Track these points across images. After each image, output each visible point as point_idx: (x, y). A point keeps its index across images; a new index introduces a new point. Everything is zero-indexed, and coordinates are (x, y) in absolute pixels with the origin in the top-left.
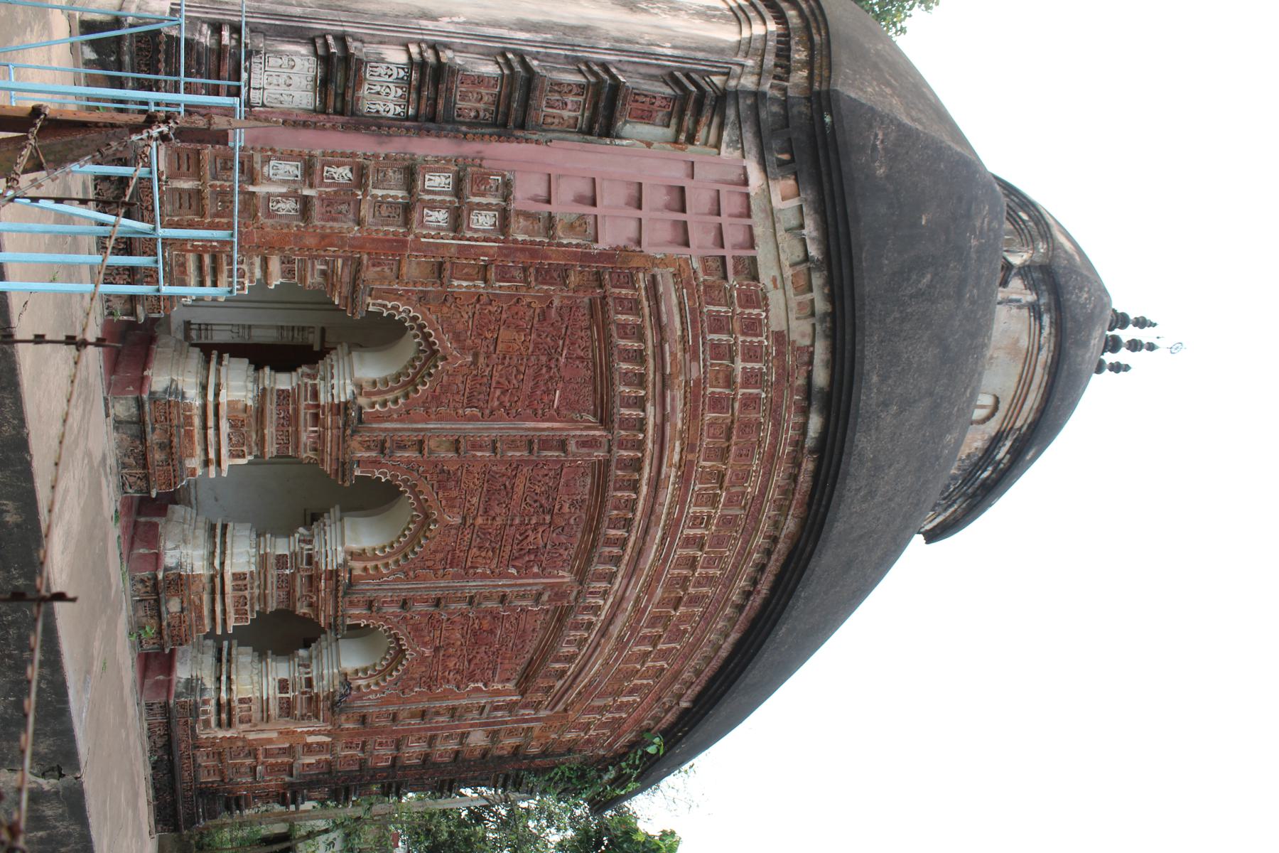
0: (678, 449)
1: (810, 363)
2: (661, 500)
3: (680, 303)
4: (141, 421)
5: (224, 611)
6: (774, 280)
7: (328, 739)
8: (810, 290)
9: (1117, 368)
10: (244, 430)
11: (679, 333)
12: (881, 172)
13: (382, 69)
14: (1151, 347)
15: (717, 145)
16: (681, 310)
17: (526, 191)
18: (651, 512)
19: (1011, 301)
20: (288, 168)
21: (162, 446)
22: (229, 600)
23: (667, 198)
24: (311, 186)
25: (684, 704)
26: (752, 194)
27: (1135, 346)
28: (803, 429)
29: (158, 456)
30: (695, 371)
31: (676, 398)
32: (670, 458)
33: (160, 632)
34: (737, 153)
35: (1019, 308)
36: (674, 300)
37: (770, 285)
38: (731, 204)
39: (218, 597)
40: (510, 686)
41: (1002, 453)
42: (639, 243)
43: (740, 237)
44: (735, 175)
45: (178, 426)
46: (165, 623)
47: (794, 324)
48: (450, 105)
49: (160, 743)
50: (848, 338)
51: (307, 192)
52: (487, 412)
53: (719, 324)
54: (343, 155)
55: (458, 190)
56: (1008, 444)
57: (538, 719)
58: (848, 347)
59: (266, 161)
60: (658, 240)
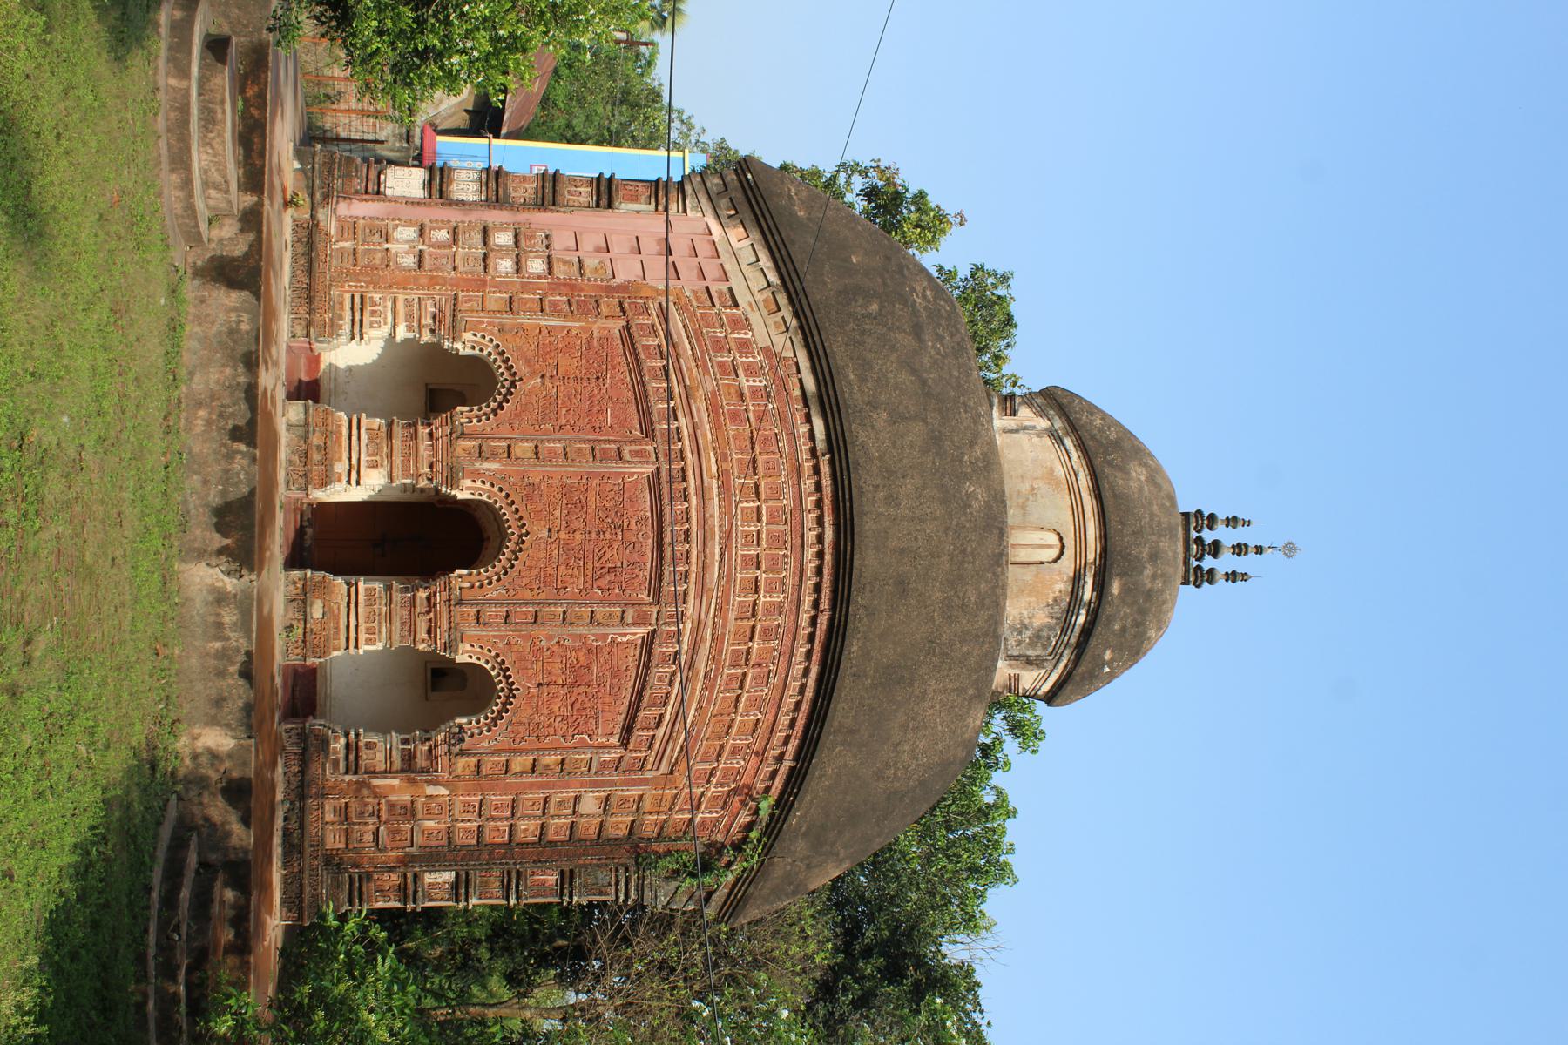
0: (713, 460)
1: (799, 372)
4: (307, 424)
7: (443, 791)
9: (1232, 577)
12: (801, 214)
13: (464, 174)
14: (1259, 550)
15: (685, 211)
17: (563, 241)
18: (704, 521)
19: (1026, 428)
21: (318, 448)
25: (788, 764)
27: (1239, 549)
29: (316, 457)
30: (710, 384)
31: (700, 407)
32: (709, 469)
38: (704, 249)
40: (614, 740)
41: (1087, 593)
43: (717, 273)
44: (701, 228)
47: (774, 338)
48: (507, 195)
50: (817, 338)
53: (719, 346)
55: (517, 244)
56: (1090, 581)
57: (645, 782)
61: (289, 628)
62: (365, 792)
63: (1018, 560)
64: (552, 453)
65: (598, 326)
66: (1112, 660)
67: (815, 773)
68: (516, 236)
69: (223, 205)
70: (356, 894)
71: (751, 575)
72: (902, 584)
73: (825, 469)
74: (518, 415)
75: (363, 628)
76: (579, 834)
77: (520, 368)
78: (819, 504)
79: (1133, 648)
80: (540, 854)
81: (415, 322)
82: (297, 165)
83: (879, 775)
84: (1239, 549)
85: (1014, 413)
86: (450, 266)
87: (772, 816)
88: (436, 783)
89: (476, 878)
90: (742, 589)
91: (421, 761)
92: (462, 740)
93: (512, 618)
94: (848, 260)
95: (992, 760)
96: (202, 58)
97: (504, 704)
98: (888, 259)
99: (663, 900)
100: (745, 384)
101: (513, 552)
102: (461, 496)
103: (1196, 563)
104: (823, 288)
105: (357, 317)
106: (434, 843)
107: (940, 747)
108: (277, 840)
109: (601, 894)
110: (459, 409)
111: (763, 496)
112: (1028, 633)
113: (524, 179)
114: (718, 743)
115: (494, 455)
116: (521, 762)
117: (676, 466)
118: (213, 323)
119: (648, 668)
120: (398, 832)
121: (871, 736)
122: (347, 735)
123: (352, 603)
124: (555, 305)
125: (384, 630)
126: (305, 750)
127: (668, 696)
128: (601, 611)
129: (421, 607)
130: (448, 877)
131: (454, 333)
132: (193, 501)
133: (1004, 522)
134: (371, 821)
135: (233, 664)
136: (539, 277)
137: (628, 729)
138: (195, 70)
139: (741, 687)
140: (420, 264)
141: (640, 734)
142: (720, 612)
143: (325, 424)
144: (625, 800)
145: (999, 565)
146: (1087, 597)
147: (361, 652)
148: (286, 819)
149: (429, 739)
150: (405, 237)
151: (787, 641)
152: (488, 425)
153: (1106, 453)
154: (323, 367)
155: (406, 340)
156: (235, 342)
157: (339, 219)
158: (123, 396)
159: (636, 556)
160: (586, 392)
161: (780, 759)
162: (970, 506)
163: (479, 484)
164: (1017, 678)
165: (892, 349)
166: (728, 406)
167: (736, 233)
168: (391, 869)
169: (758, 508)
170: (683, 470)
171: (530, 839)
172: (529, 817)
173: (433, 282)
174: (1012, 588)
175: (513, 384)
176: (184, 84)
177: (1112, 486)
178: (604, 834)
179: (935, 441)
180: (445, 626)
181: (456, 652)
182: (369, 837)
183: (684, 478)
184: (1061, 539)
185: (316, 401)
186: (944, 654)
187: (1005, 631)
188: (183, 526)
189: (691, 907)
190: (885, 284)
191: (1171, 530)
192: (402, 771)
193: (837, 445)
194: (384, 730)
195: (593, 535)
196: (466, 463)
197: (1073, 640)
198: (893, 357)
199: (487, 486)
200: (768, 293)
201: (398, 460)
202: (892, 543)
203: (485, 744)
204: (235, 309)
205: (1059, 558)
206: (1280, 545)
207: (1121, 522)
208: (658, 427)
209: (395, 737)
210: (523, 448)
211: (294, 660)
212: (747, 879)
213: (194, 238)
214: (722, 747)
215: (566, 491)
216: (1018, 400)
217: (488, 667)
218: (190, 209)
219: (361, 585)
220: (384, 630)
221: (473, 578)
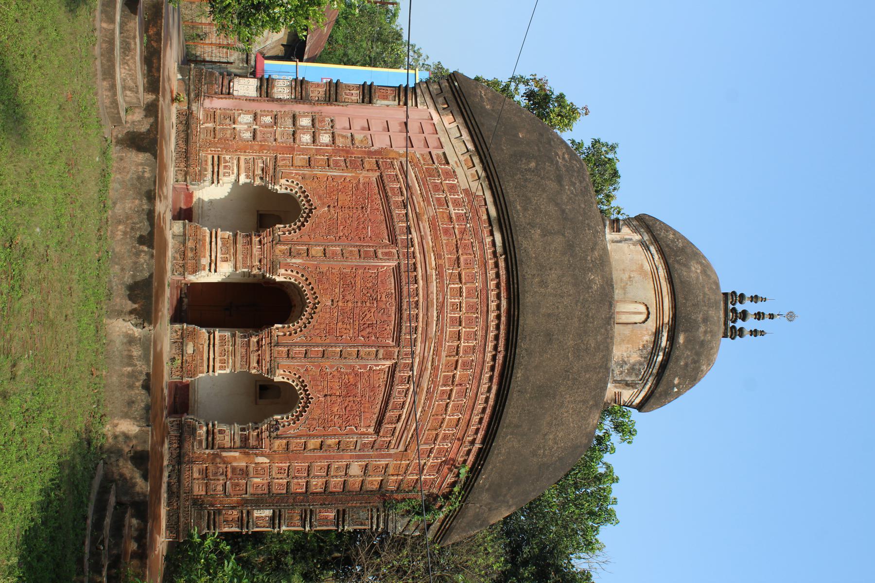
0: (433, 258)
1: (486, 204)
4: (185, 235)
6: (456, 163)
7: (266, 460)
8: (474, 166)
9: (754, 333)
12: (488, 107)
13: (281, 82)
14: (772, 316)
15: (416, 105)
17: (341, 124)
18: (427, 296)
19: (626, 240)
21: (192, 249)
22: (216, 349)
25: (478, 446)
27: (759, 316)
28: (494, 243)
29: (190, 255)
31: (425, 226)
32: (430, 264)
35: (634, 245)
37: (455, 166)
38: (428, 128)
39: (211, 346)
40: (371, 430)
41: (664, 342)
43: (436, 144)
44: (427, 116)
48: (307, 95)
50: (497, 183)
51: (255, 127)
53: (437, 188)
55: (313, 125)
56: (665, 334)
57: (390, 456)
58: (499, 189)
61: (173, 360)
62: (218, 460)
63: (621, 321)
64: (334, 254)
65: (363, 175)
66: (679, 384)
67: (494, 451)
68: (313, 120)
69: (135, 101)
70: (212, 523)
71: (456, 329)
72: (549, 335)
73: (502, 264)
74: (314, 230)
75: (218, 359)
76: (348, 488)
77: (315, 201)
78: (498, 286)
79: (692, 377)
80: (326, 499)
82: (180, 77)
83: (534, 454)
84: (759, 316)
85: (619, 230)
86: (272, 139)
87: (467, 478)
88: (262, 455)
89: (285, 514)
90: (450, 338)
91: (252, 442)
92: (278, 429)
93: (309, 355)
94: (516, 135)
95: (603, 446)
96: (122, 11)
97: (304, 407)
98: (541, 135)
99: (400, 529)
100: (453, 212)
101: (310, 314)
102: (278, 279)
103: (731, 324)
104: (501, 153)
105: (216, 170)
106: (260, 492)
107: (571, 436)
108: (164, 487)
109: (362, 524)
110: (278, 226)
111: (464, 281)
112: (627, 367)
113: (318, 85)
114: (435, 432)
115: (299, 254)
116: (313, 443)
117: (411, 262)
118: (128, 173)
119: (392, 386)
120: (237, 485)
121: (530, 429)
122: (207, 425)
123: (211, 344)
124: (336, 163)
125: (230, 361)
126: (181, 434)
128: (364, 350)
129: (253, 347)
130: (268, 513)
131: (275, 180)
132: (115, 281)
133: (612, 298)
134: (221, 478)
135: (138, 380)
136: (327, 146)
137: (379, 423)
138: (118, 18)
139: (449, 398)
141: (386, 427)
142: (437, 352)
143: (196, 235)
144: (377, 467)
145: (609, 324)
146: (663, 344)
147: (216, 374)
148: (169, 476)
149: (257, 428)
150: (245, 121)
151: (478, 370)
152: (295, 236)
153: (676, 255)
154: (194, 200)
155: (245, 184)
156: (141, 184)
157: (205, 110)
158: (73, 216)
159: (385, 317)
160: (355, 216)
161: (473, 442)
162: (591, 288)
163: (289, 272)
164: (620, 394)
165: (544, 190)
166: (442, 225)
167: (448, 119)
168: (233, 508)
169: (461, 288)
170: (415, 264)
172: (318, 476)
173: (262, 148)
174: (617, 339)
175: (311, 211)
176: (111, 26)
177: (679, 277)
178: (364, 488)
179: (570, 247)
180: (268, 359)
181: (275, 375)
182: (220, 488)
183: (415, 269)
184: (648, 309)
185: (190, 220)
186: (574, 379)
187: (613, 365)
188: (109, 296)
189: (417, 534)
190: (539, 150)
191: (716, 303)
192: (241, 447)
193: (510, 250)
194: (230, 423)
195: (359, 304)
196: (281, 259)
197: (655, 371)
198: (544, 195)
199: (294, 273)
200: (467, 156)
201: (240, 257)
202: (543, 310)
203: (292, 432)
204: (141, 164)
205: (646, 320)
206: (785, 313)
207: (685, 299)
208: (399, 238)
210: (317, 251)
211: (176, 379)
212: (452, 517)
213: (117, 121)
214: (437, 435)
215: (343, 277)
216: (621, 223)
217: (294, 384)
218: (115, 103)
219: (217, 333)
220: (230, 361)
221: (286, 330)
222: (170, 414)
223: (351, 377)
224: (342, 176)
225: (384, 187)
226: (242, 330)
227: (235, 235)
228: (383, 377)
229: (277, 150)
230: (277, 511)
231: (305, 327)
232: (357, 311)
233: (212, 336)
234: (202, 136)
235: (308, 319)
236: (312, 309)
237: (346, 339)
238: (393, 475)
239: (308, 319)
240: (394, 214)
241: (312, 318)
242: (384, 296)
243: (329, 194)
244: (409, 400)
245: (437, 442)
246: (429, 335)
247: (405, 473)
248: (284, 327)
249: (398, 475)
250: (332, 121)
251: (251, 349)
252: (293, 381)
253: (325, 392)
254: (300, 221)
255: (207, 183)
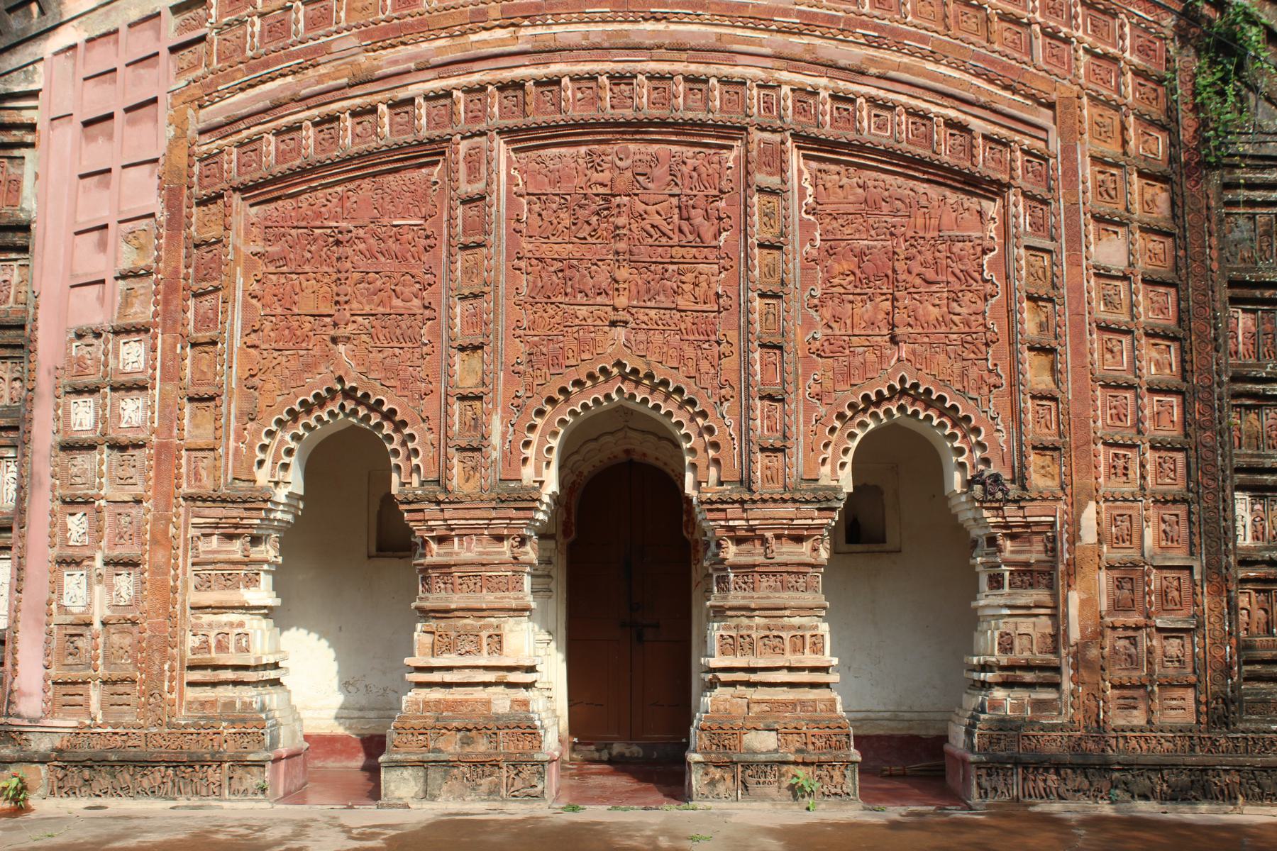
0: (484, 35)
2: (576, 40)
3: (242, 90)
4: (423, 764)
5: (791, 669)
10: (453, 634)
11: (289, 79)
15: (34, 94)
16: (251, 86)
17: (91, 310)
20: (72, 585)
21: (466, 742)
22: (761, 664)
23: (100, 140)
24: (92, 558)
26: (86, 36)
29: (482, 746)
31: (387, 60)
32: (502, 42)
33: (805, 764)
34: (40, 66)
36: (241, 96)
38: (102, 58)
42: (156, 161)
43: (146, 32)
45: (438, 719)
46: (792, 758)
48: (8, 411)
49: (1081, 781)
51: (98, 563)
52: (427, 312)
54: (53, 525)
55: (93, 390)
57: (1068, 151)
59: (62, 608)
60: (152, 137)
61: (796, 792)
62: (1093, 653)
64: (475, 320)
68: (78, 392)
75: (785, 655)
81: (246, 570)
86: (134, 511)
88: (1075, 524)
91: (1035, 553)
92: (996, 478)
97: (928, 405)
101: (653, 389)
102: (552, 484)
106: (1184, 525)
110: (395, 489)
114: (997, 25)
115: (477, 424)
116: (1036, 374)
119: (862, 147)
120: (1164, 594)
122: (985, 686)
123: (749, 678)
124: (204, 321)
125: (796, 621)
127: (913, 113)
128: (759, 231)
129: (754, 554)
130: (1243, 506)
131: (257, 501)
134: (1144, 643)
140: (131, 564)
141: (983, 162)
147: (835, 661)
148: (1145, 797)
149: (992, 541)
150: (82, 592)
154: (340, 731)
155: (277, 588)
157: (49, 713)
160: (363, 264)
163: (530, 452)
168: (1233, 608)
170: (502, 87)
171: (1173, 357)
173: (161, 540)
175: (349, 394)
178: (1164, 225)
180: (788, 510)
181: (837, 490)
182: (1173, 647)
183: (518, 85)
192: (1051, 586)
194: (971, 621)
195: (622, 246)
196: (493, 475)
199: (534, 437)
201: (487, 599)
208: (424, 134)
209: (986, 599)
210: (465, 372)
211: (851, 782)
215: (542, 297)
217: (861, 434)
219: (715, 662)
220: (796, 621)
221: (701, 460)
222: (958, 798)
223: (837, 268)
224: (246, 306)
225: (275, 180)
226: (696, 595)
227: (425, 614)
228: (835, 175)
229: (168, 496)
230: (1239, 478)
231: (692, 402)
232: (643, 253)
233: (723, 677)
234: (128, 719)
235: (668, 396)
236: (638, 383)
237: (726, 283)
238: (1125, 143)
239: (668, 396)
240: (355, 149)
241: (665, 383)
242: (597, 177)
243: (298, 340)
244: (904, 99)
245: (1026, 16)
246: (712, 41)
247: (1117, 108)
248: (694, 466)
249: (1124, 128)
250: (80, 336)
251: (760, 559)
252: (852, 436)
253: (883, 341)
254: (379, 426)
255: (272, 698)
